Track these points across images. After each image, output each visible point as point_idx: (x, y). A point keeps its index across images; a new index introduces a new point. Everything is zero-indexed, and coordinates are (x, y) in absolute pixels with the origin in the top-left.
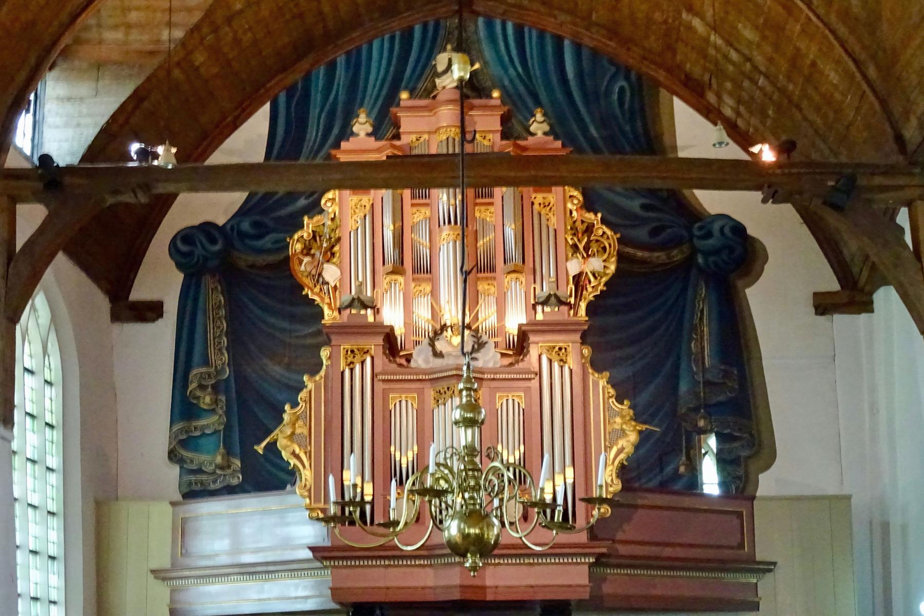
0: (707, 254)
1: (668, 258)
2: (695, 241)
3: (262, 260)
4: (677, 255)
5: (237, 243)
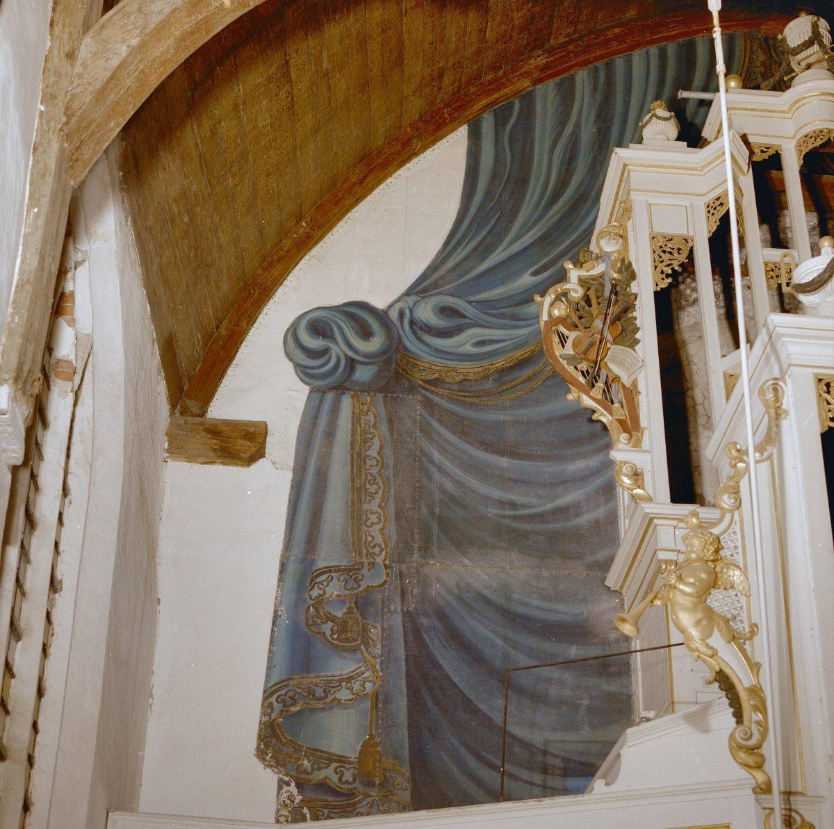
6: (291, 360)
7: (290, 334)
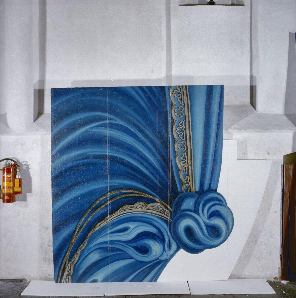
3: (139, 209)
5: (164, 227)
6: (229, 209)
7: (231, 227)
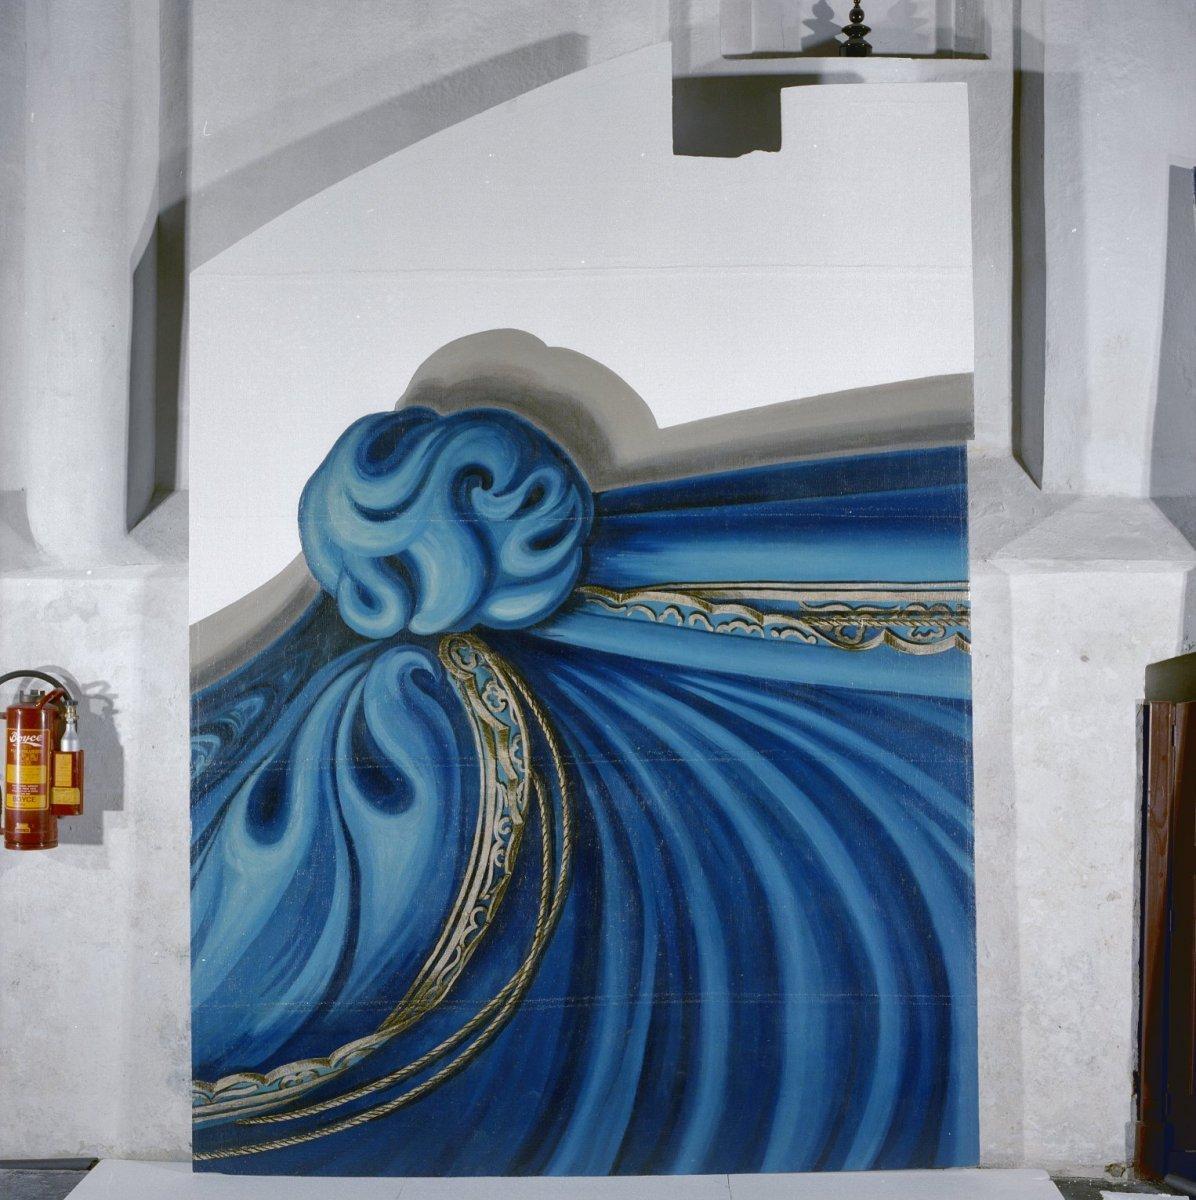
0: (491, 580)
1: (508, 736)
2: (421, 626)
4: (493, 699)
